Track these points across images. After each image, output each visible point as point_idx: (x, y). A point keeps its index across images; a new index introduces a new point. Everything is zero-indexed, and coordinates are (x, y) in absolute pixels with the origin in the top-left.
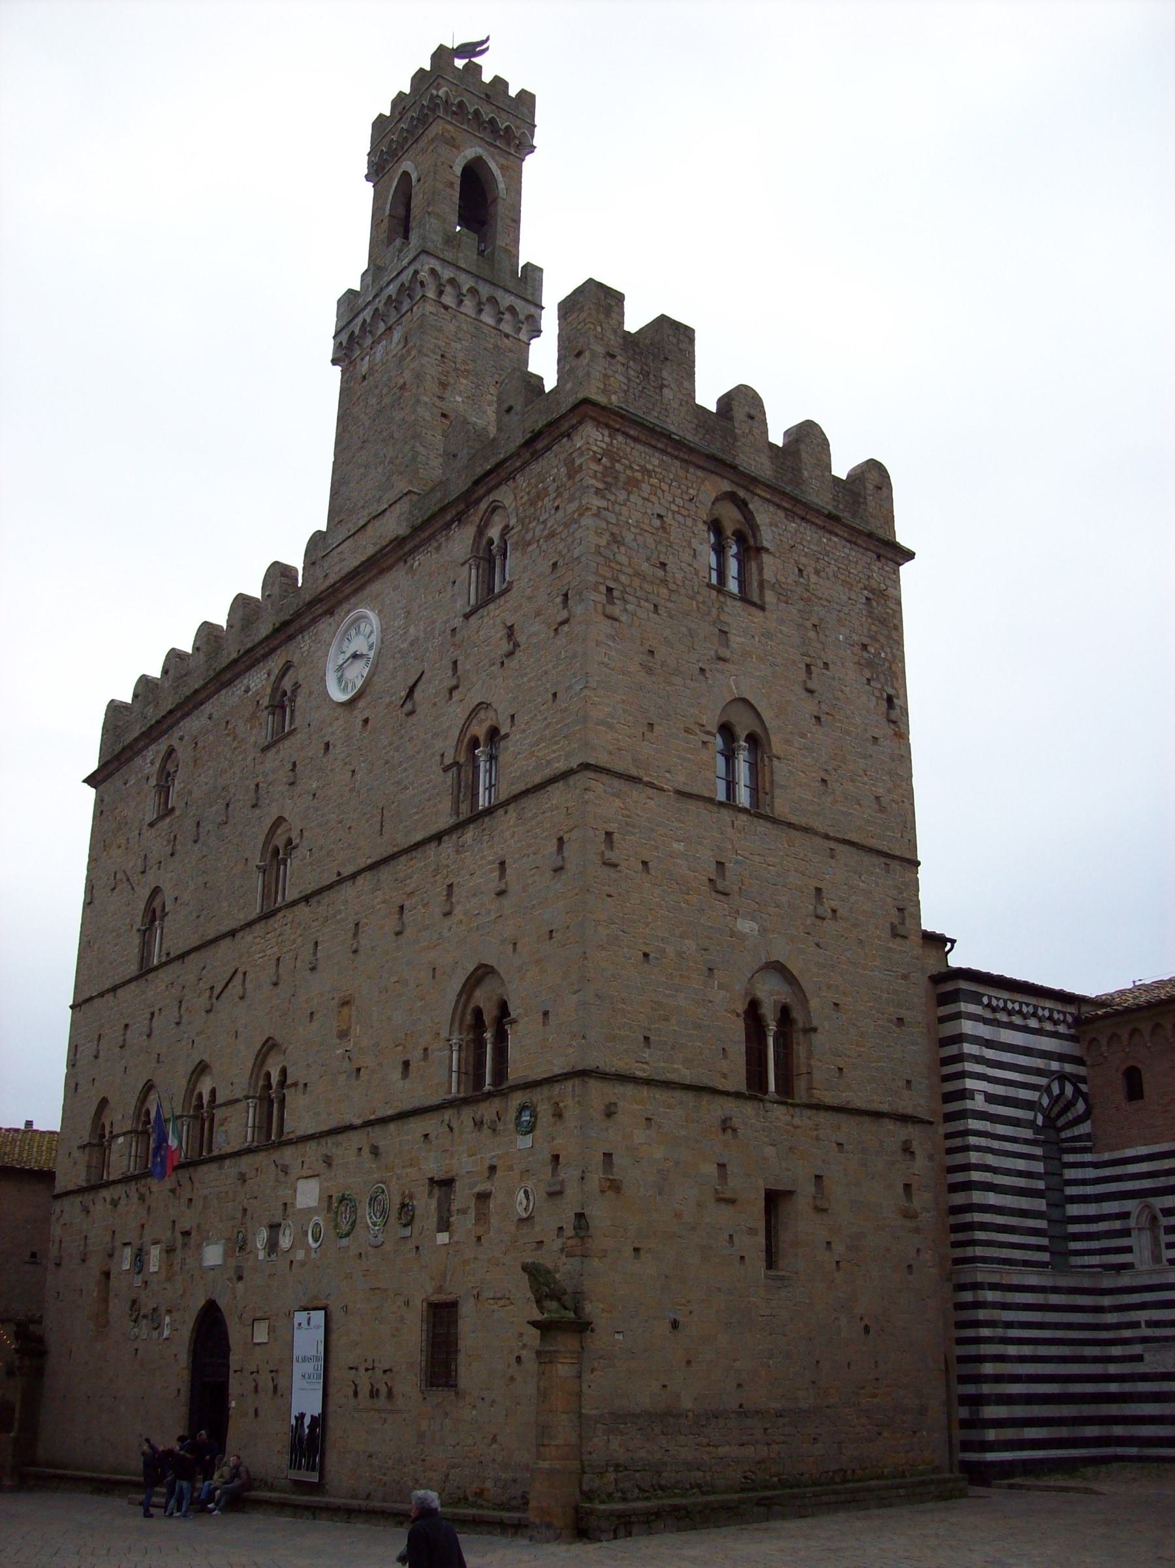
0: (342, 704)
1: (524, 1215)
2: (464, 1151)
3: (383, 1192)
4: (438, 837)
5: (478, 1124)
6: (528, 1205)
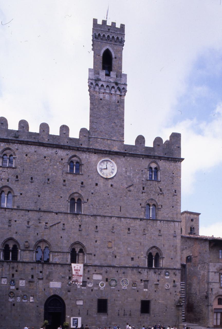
0: (102, 177)
1: (167, 289)
2: (152, 276)
3: (126, 280)
4: (141, 220)
5: (155, 273)
6: (168, 287)
